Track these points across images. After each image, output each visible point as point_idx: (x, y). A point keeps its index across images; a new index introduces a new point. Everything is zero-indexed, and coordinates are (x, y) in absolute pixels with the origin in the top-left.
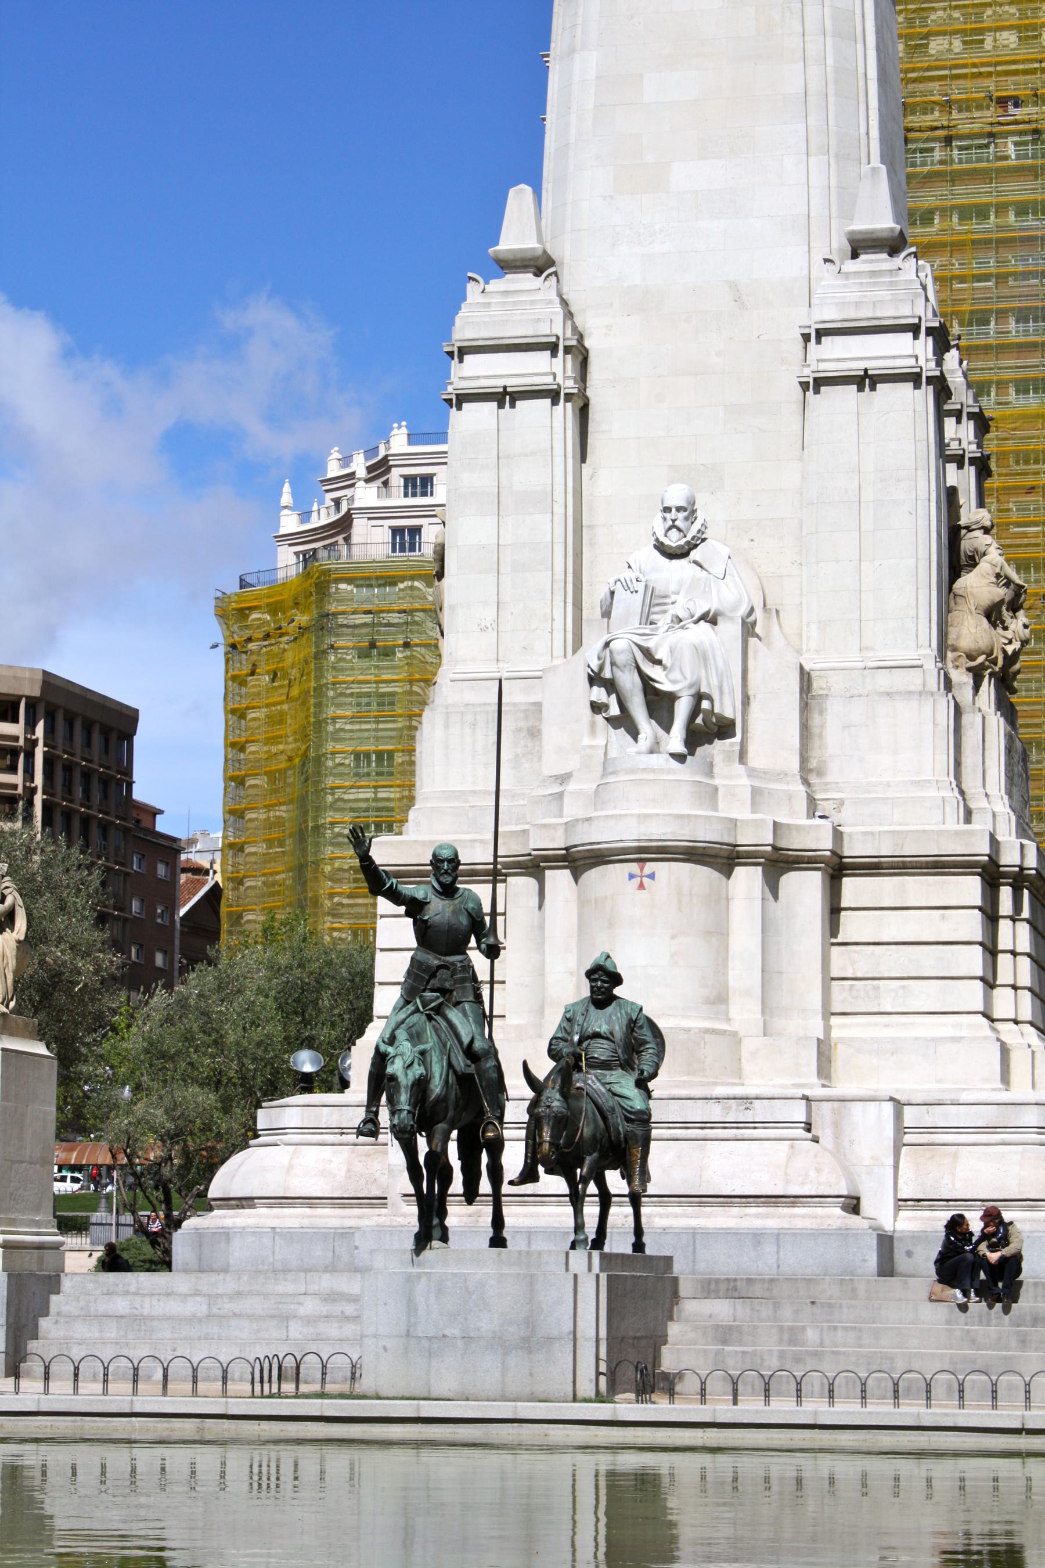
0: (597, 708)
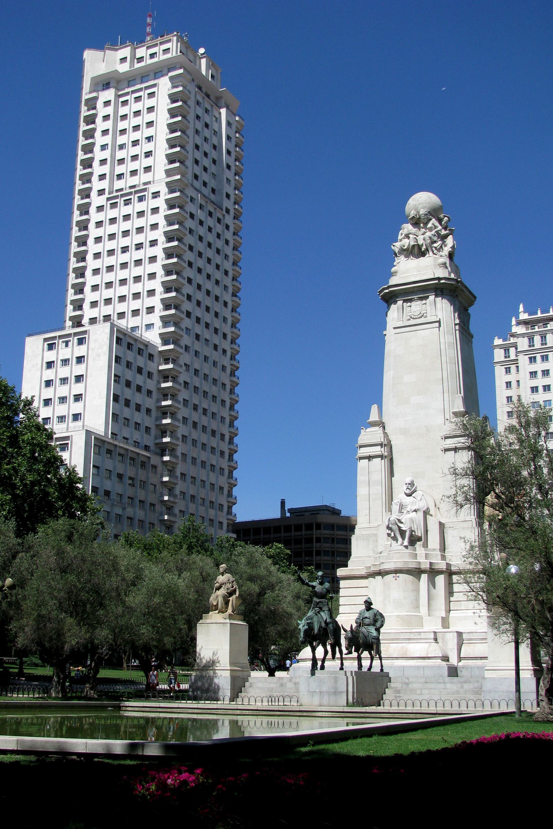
0: (389, 535)
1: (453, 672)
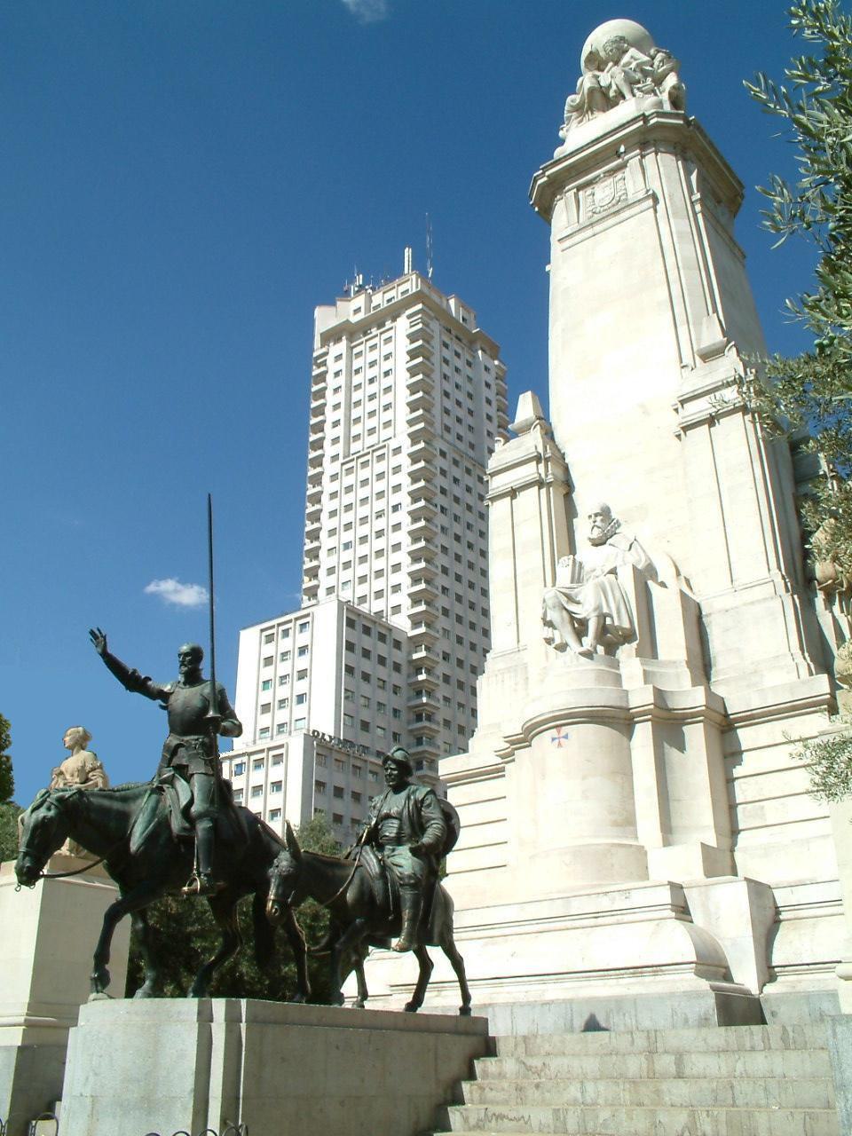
1: (739, 1010)
